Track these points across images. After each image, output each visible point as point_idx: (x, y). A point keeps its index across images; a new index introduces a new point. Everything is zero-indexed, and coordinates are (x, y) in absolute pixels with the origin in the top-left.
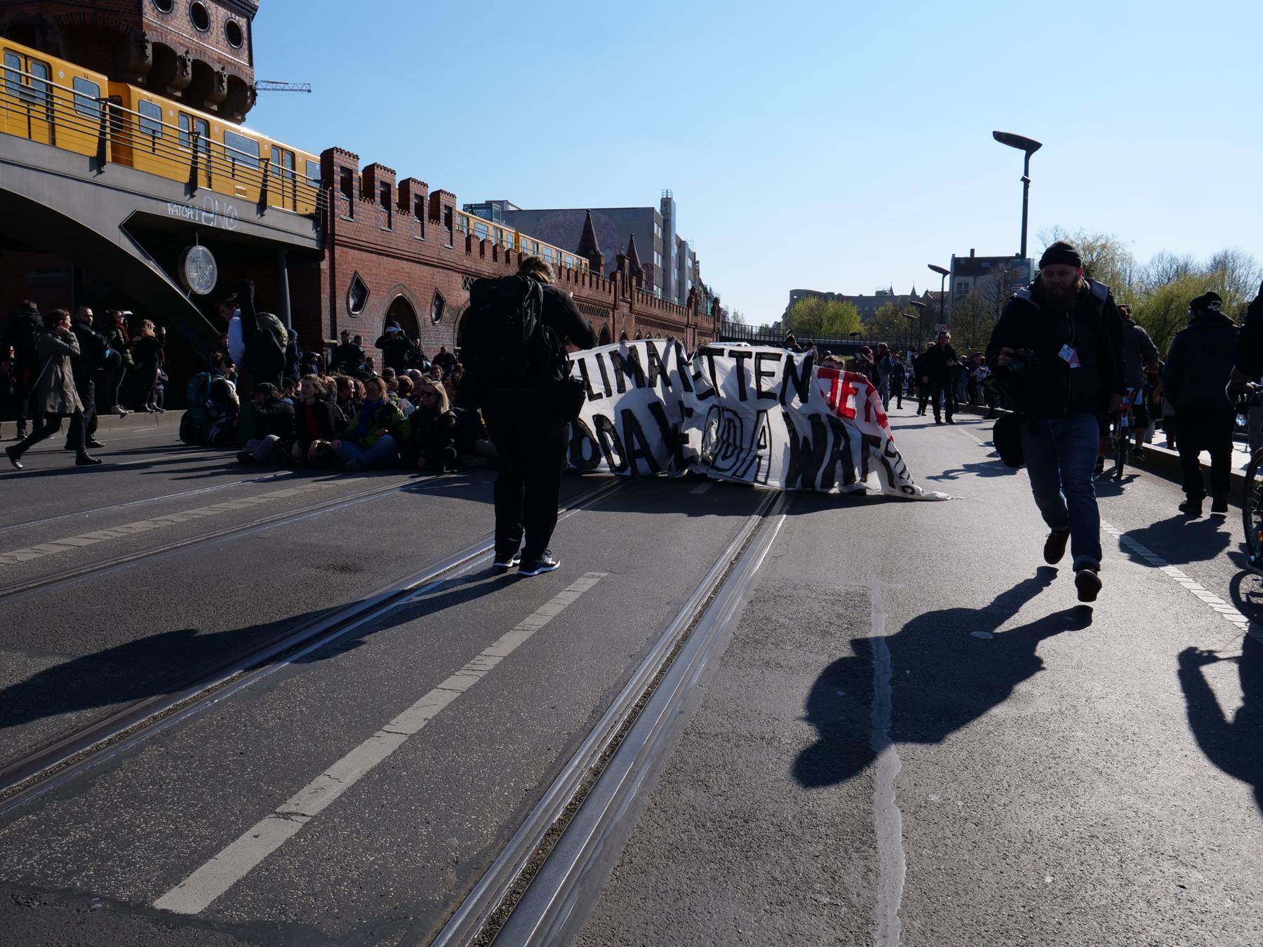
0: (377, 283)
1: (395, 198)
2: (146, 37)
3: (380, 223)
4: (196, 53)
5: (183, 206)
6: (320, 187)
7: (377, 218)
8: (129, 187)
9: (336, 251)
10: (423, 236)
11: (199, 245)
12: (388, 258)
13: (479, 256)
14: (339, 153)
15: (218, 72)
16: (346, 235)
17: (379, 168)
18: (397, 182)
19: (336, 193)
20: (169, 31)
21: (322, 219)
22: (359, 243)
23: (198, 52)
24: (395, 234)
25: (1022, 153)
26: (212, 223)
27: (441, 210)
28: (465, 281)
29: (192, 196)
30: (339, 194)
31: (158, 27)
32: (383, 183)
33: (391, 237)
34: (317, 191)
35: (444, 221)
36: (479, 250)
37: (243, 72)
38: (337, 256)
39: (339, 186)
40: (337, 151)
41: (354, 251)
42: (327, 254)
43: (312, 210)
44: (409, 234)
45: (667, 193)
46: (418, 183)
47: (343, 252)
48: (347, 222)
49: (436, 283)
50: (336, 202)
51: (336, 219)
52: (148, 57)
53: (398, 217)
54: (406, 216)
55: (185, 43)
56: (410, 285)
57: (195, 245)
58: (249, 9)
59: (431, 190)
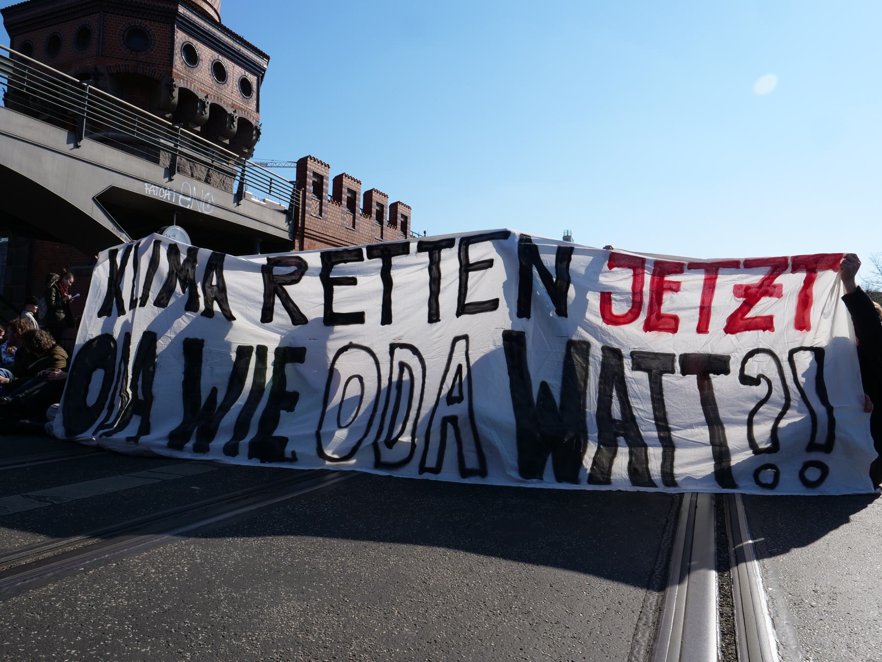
1: (360, 203)
2: (174, 83)
3: (345, 222)
4: (214, 98)
5: (161, 187)
7: (343, 219)
8: (107, 164)
9: (305, 243)
11: (176, 225)
14: (312, 161)
15: (230, 115)
17: (347, 178)
19: (307, 194)
20: (194, 80)
21: (294, 214)
22: (326, 237)
23: (216, 98)
24: (358, 233)
26: (189, 206)
29: (171, 180)
31: (185, 76)
32: (349, 190)
34: (292, 190)
35: (400, 227)
37: (251, 115)
39: (312, 188)
40: (311, 159)
41: (321, 244)
43: (286, 206)
44: (370, 235)
47: (311, 244)
48: (316, 219)
50: (307, 201)
51: (307, 215)
52: (174, 98)
53: (361, 219)
55: (206, 90)
57: (172, 224)
58: (259, 70)
59: (390, 201)
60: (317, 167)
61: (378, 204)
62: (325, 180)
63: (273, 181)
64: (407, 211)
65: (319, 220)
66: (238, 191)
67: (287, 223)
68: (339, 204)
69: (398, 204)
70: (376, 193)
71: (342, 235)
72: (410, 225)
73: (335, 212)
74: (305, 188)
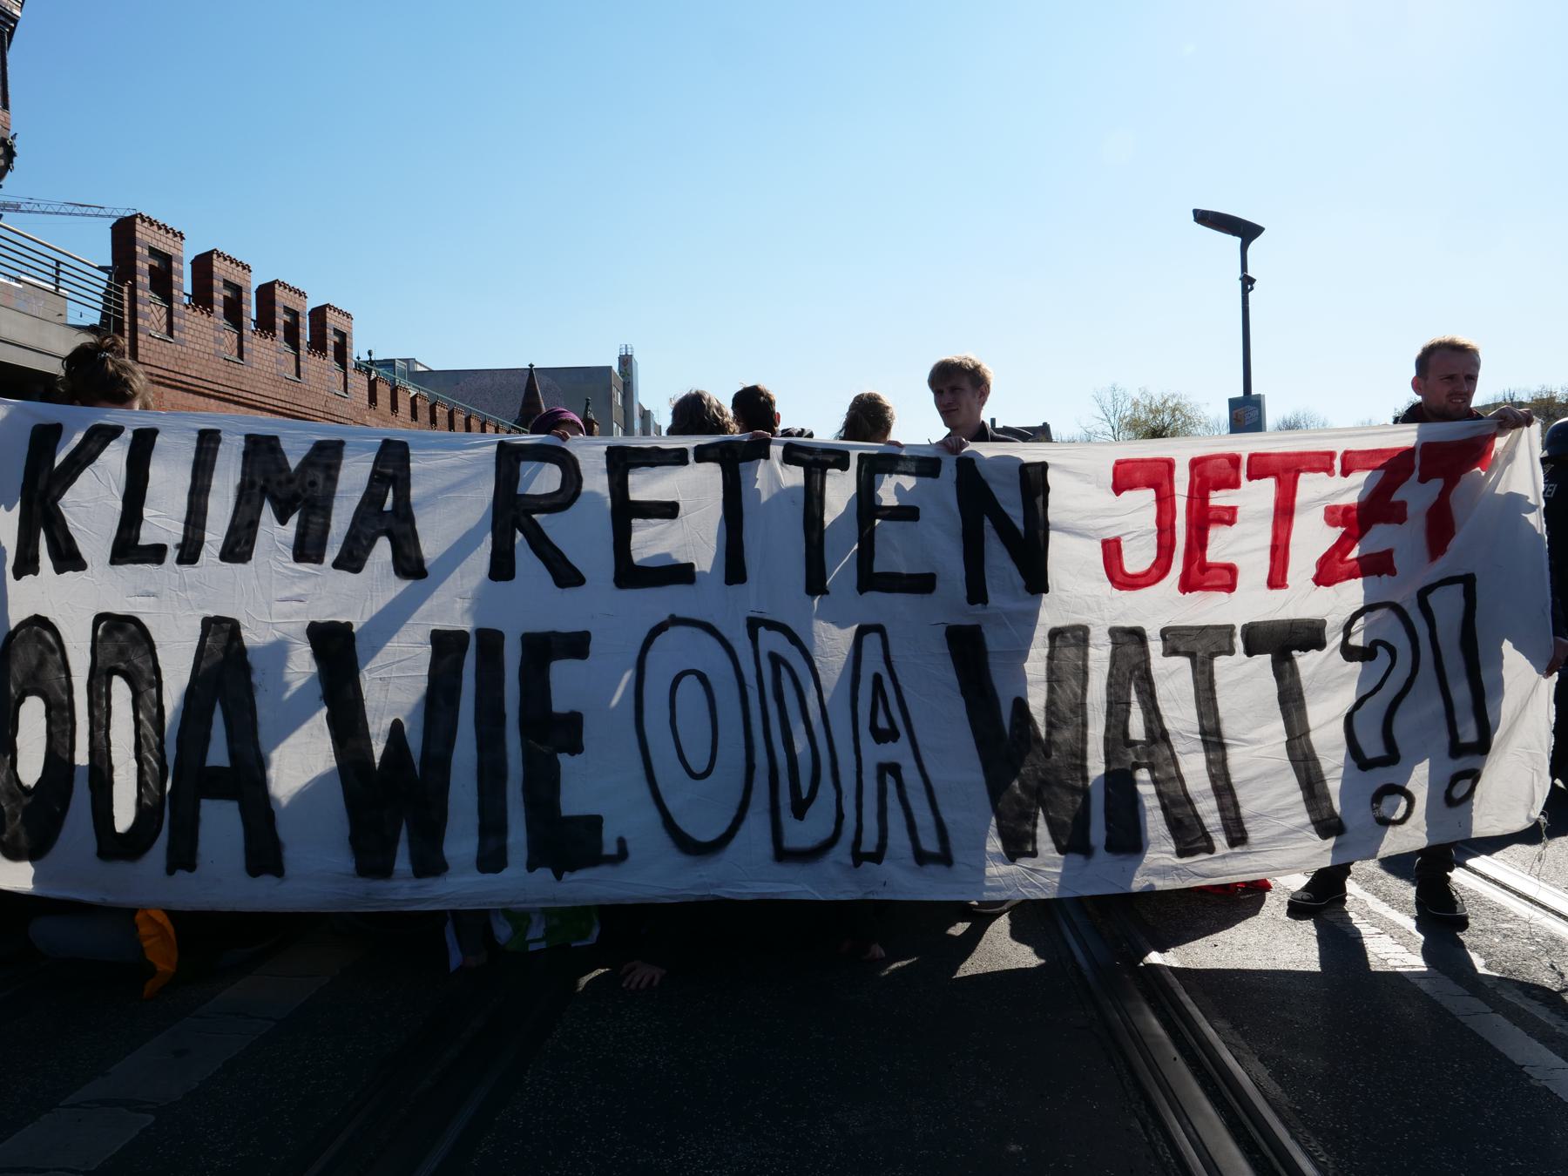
1: (251, 310)
3: (222, 348)
6: (110, 278)
7: (217, 341)
10: (298, 375)
12: (237, 407)
13: (389, 411)
14: (146, 224)
16: (159, 365)
17: (221, 259)
18: (254, 287)
19: (139, 292)
22: (184, 379)
27: (328, 336)
30: (144, 293)
33: (243, 374)
34: (104, 285)
35: (333, 354)
39: (147, 281)
41: (175, 392)
44: (275, 371)
46: (290, 290)
50: (139, 307)
51: (140, 336)
53: (255, 341)
60: (158, 237)
61: (287, 310)
62: (175, 264)
63: (62, 267)
64: (346, 323)
65: (167, 344)
68: (207, 312)
69: (328, 309)
70: (282, 288)
71: (218, 373)
72: (351, 348)
74: (134, 281)
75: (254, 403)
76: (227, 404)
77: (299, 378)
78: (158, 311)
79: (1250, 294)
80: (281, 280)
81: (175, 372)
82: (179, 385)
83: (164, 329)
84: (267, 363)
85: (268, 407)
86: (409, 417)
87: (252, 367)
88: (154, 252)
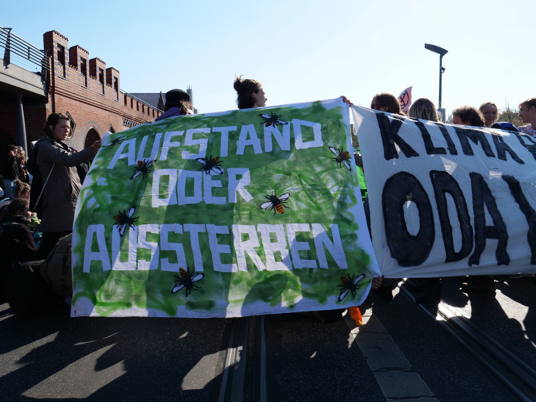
0: (80, 119)
7: (79, 80)
9: (55, 98)
10: (104, 93)
13: (131, 107)
19: (55, 60)
25: (439, 55)
28: (124, 121)
30: (56, 61)
33: (87, 92)
36: (130, 104)
38: (56, 101)
39: (57, 56)
42: (50, 99)
43: (40, 70)
44: (96, 91)
45: (189, 87)
47: (59, 98)
48: (62, 79)
49: (110, 121)
51: (56, 77)
53: (90, 80)
54: (95, 80)
56: (98, 122)
59: (107, 67)
60: (60, 40)
63: (30, 50)
64: (118, 75)
65: (64, 80)
66: (5, 56)
67: (42, 82)
69: (112, 69)
70: (98, 60)
71: (79, 92)
72: (119, 84)
73: (73, 74)
74: (53, 56)
75: (90, 103)
76: (82, 103)
77: (104, 94)
78: (60, 68)
79: (442, 74)
80: (98, 58)
81: (67, 91)
82: (67, 96)
83: (63, 75)
84: (94, 88)
85: (95, 105)
86: (136, 110)
87: (90, 90)
88: (59, 46)
